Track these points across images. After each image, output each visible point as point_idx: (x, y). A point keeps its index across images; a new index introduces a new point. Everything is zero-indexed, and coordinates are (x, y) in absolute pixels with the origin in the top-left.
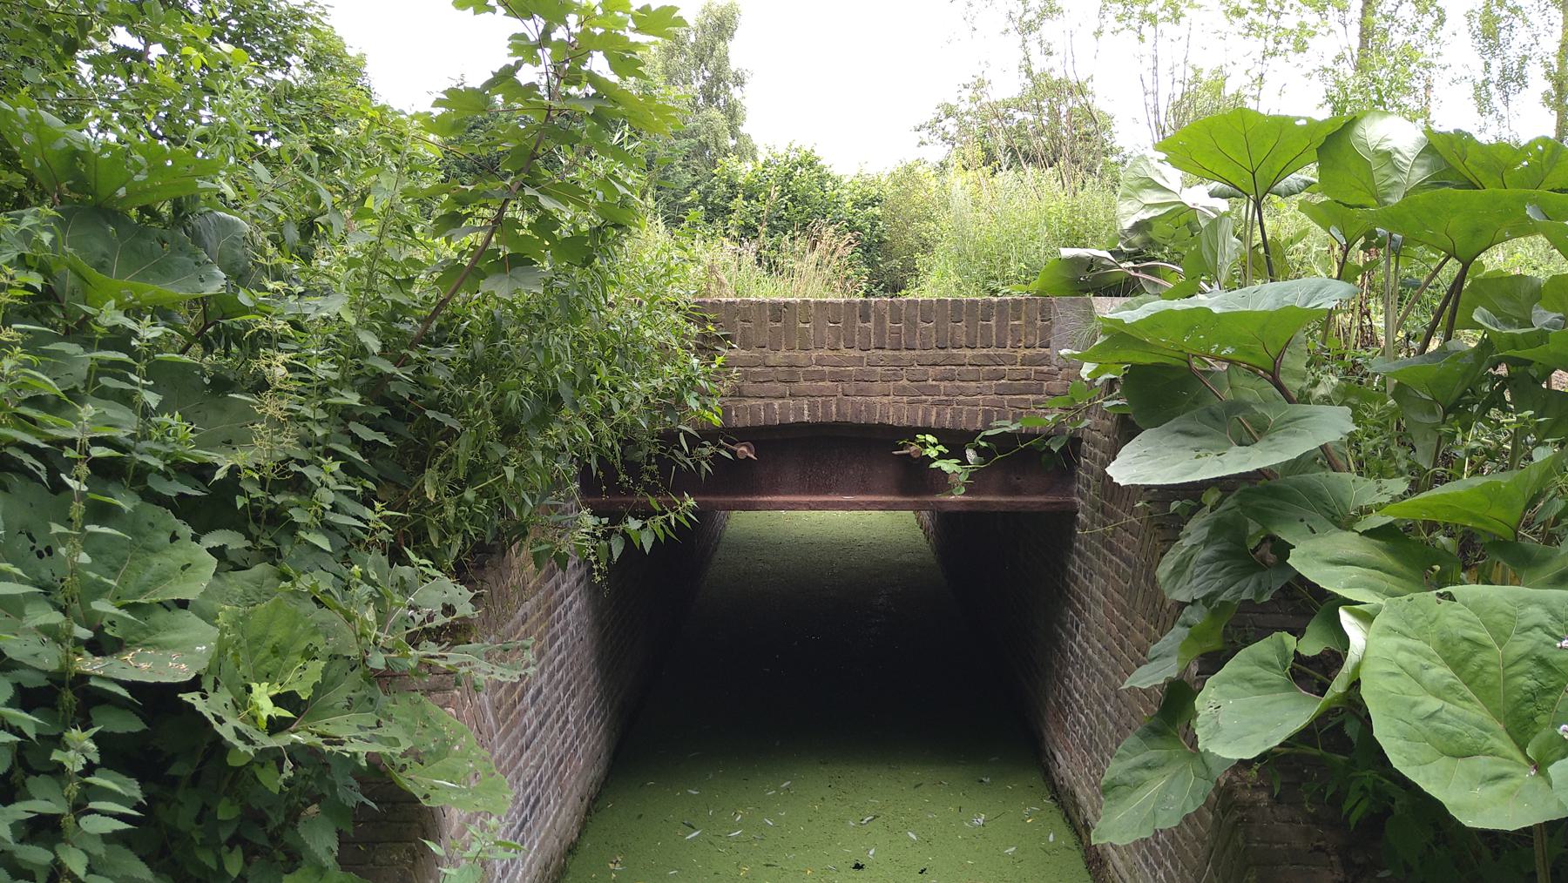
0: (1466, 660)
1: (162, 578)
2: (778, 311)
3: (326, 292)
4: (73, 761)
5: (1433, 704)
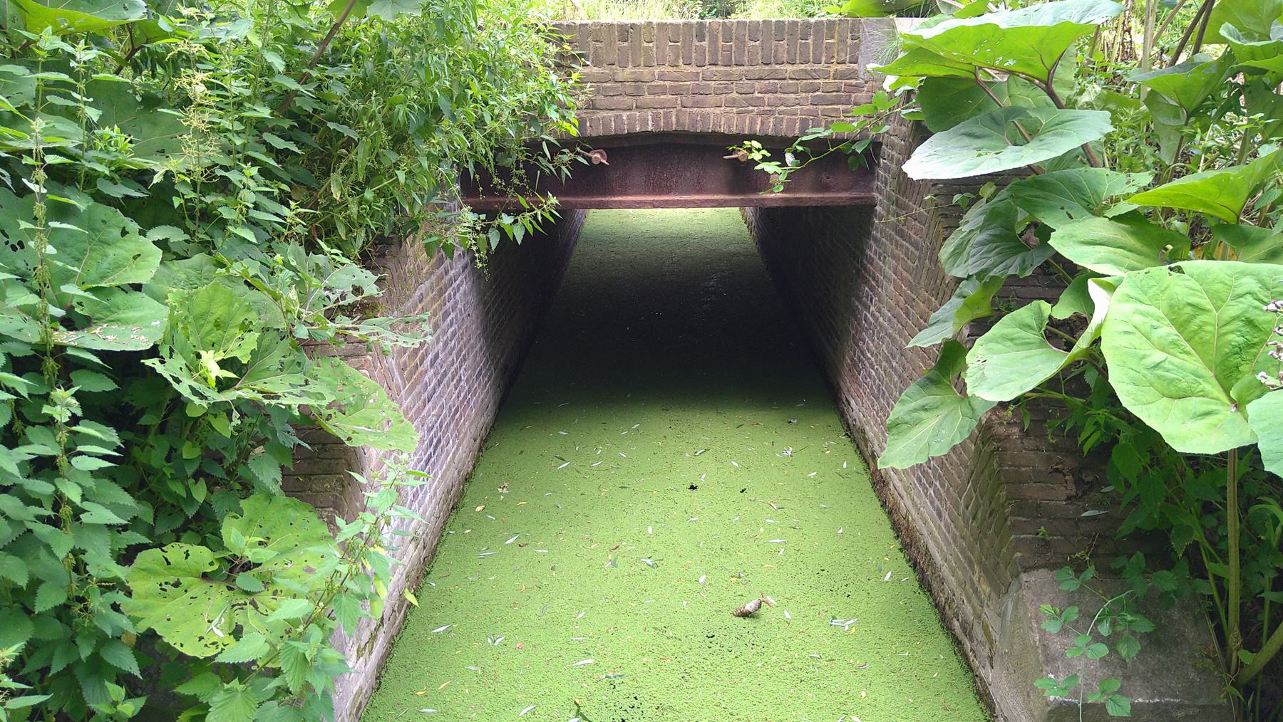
0: (1188, 321)
1: (118, 266)
2: (626, 31)
3: (234, 18)
4: (61, 415)
5: (1158, 356)
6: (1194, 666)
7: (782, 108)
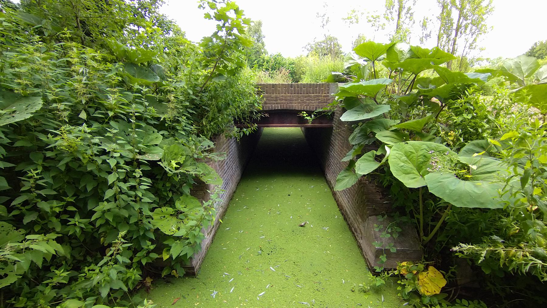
1: (152, 140)
2: (274, 86)
3: (181, 81)
4: (137, 175)
5: (402, 164)
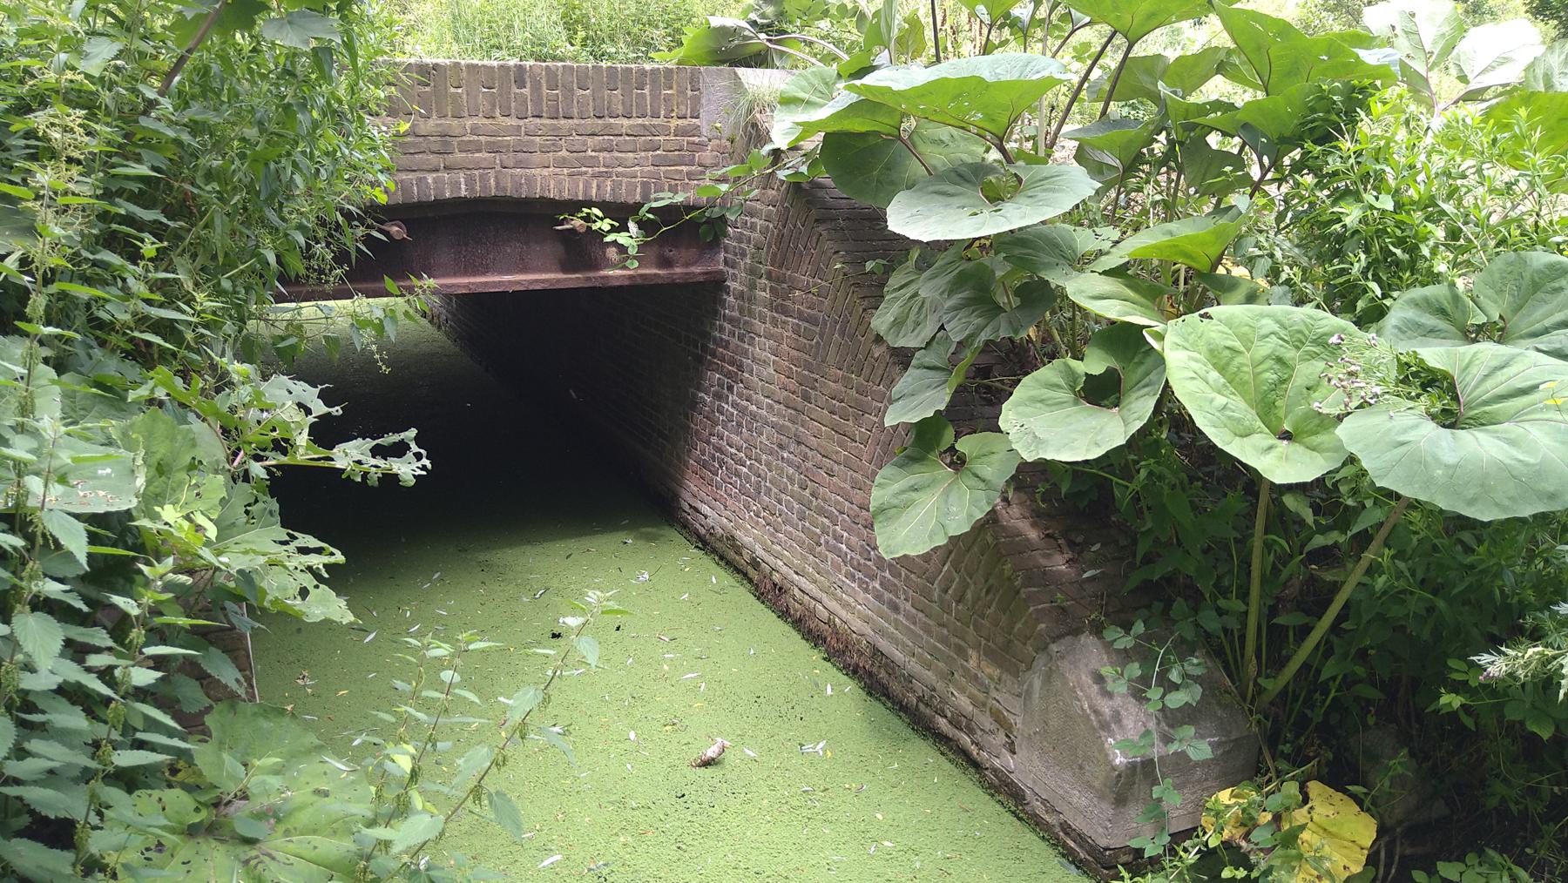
0: (1228, 364)
6: (1219, 704)
7: (620, 169)
